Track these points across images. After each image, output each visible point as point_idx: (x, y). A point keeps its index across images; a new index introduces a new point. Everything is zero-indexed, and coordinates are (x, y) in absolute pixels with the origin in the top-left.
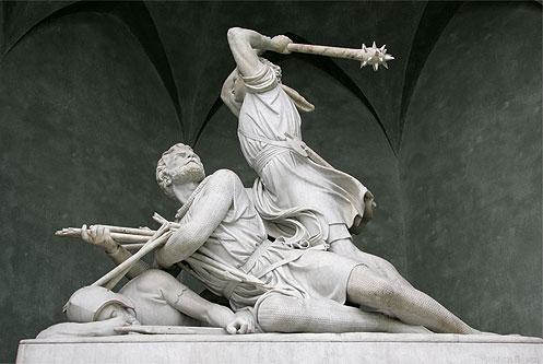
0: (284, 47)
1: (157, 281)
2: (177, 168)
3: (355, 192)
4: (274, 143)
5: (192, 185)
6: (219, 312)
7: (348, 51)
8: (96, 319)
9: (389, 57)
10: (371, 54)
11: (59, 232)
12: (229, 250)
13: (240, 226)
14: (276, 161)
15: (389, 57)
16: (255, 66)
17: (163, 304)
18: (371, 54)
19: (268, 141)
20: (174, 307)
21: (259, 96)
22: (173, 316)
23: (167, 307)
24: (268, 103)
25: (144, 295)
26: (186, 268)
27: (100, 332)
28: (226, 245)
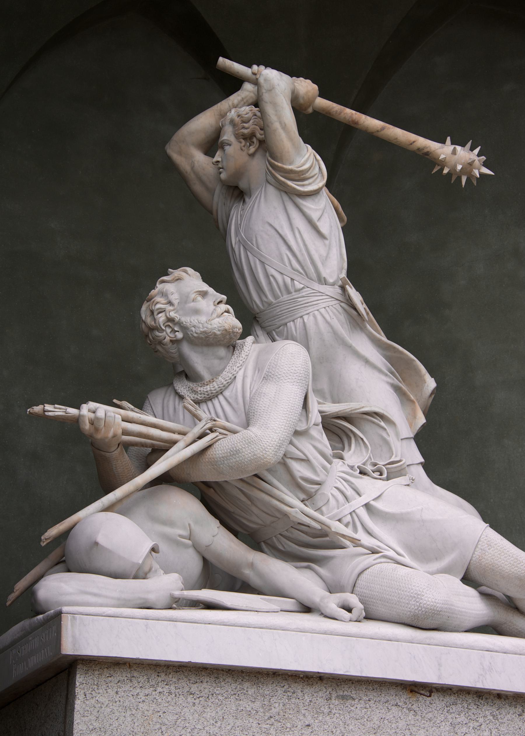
0: (311, 102)
2: (203, 319)
3: (421, 382)
4: (317, 286)
5: (222, 352)
7: (422, 142)
9: (486, 171)
12: (297, 474)
13: (312, 438)
14: (319, 317)
15: (486, 171)
17: (186, 546)
19: (306, 281)
20: (196, 547)
21: (300, 201)
23: (191, 552)
24: (315, 216)
25: (167, 530)
27: (152, 597)
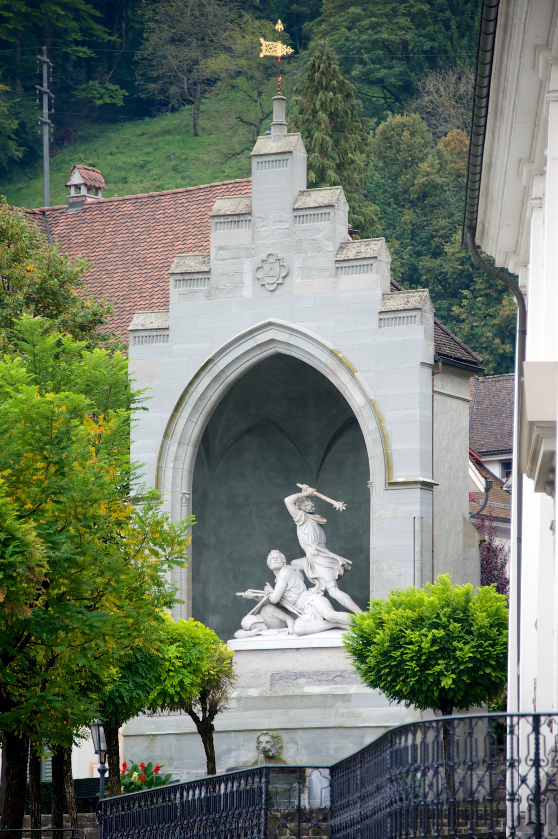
1: (270, 611)
6: (289, 621)
8: (250, 630)
10: (339, 505)
11: (238, 594)
16: (297, 515)
18: (339, 505)
22: (277, 622)
26: (279, 606)
28: (289, 599)
